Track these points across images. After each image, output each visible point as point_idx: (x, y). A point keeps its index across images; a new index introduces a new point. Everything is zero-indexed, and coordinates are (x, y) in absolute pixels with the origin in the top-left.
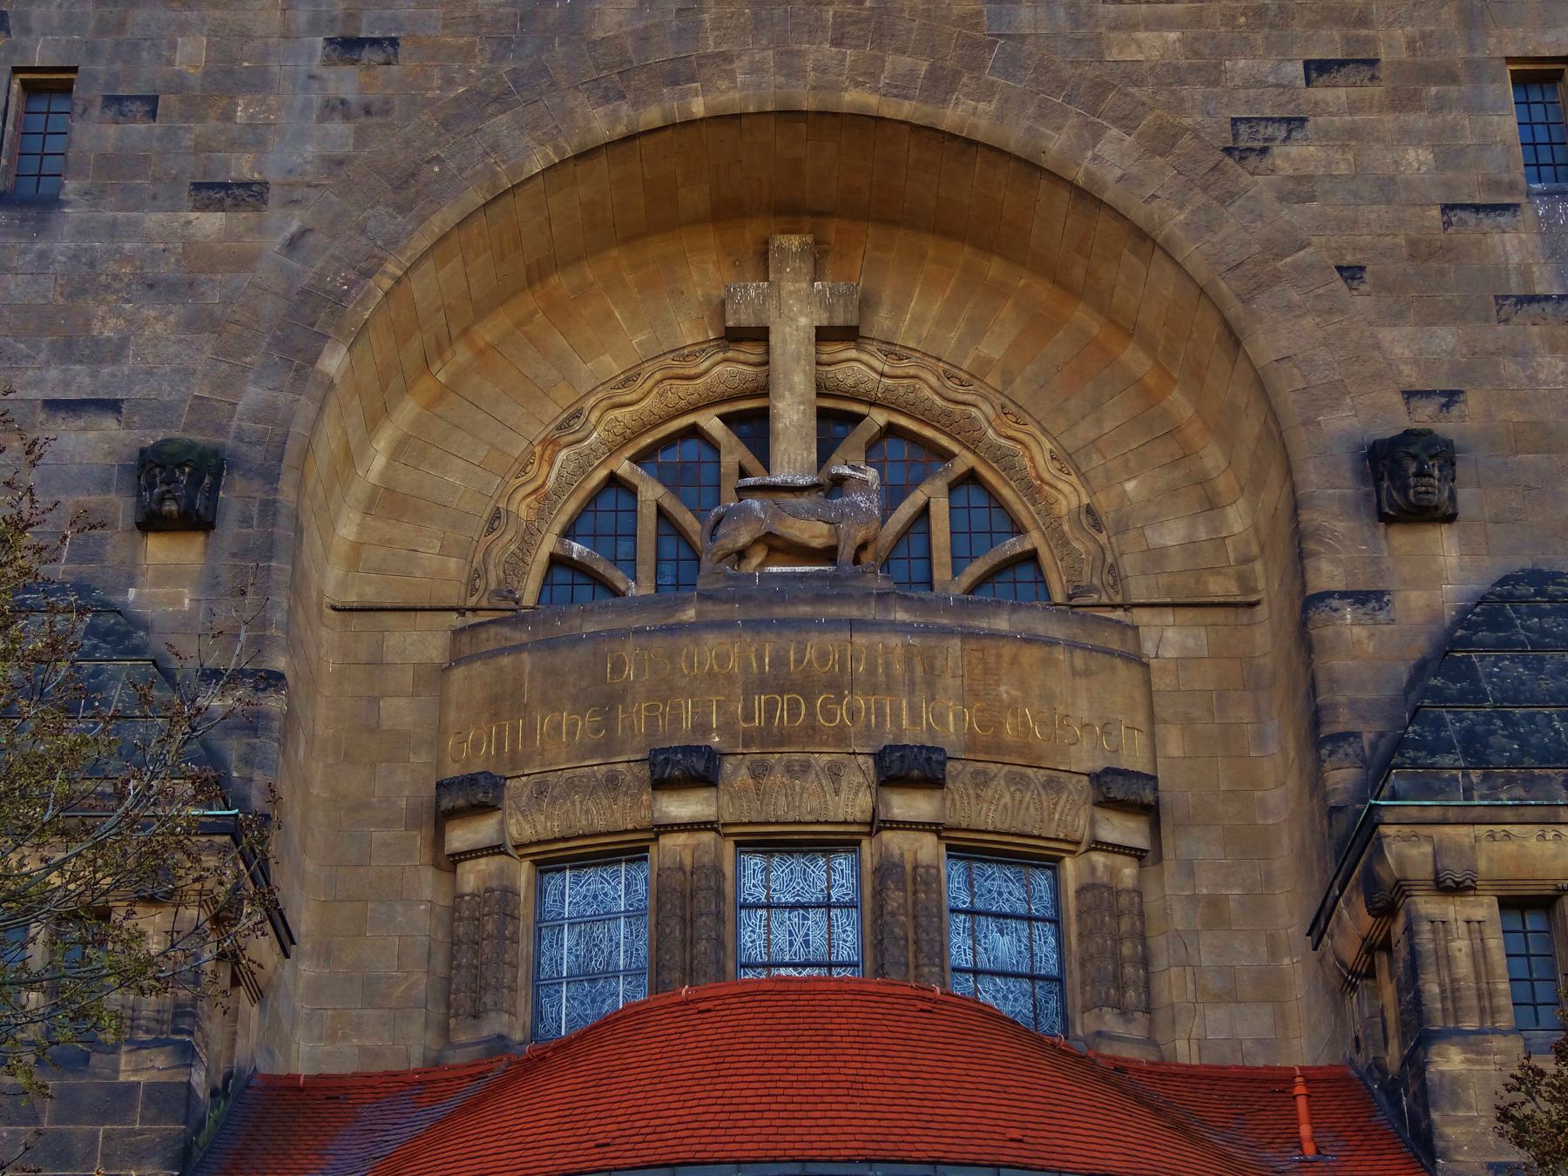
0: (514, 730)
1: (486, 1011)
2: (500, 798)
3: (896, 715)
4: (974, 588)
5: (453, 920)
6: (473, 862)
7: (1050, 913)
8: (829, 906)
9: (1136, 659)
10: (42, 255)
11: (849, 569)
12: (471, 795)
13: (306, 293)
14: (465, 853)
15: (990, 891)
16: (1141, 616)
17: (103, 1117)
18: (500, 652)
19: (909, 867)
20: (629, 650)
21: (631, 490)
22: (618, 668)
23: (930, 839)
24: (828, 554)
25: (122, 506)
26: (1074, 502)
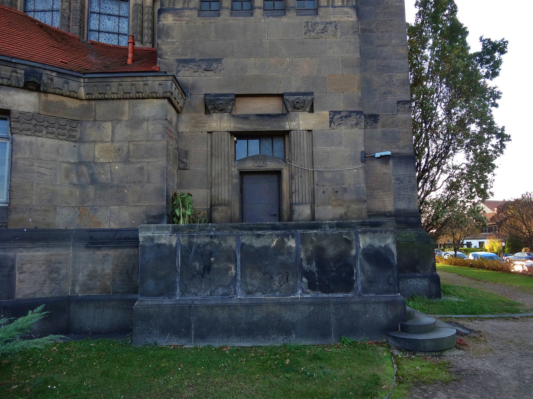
7: (126, 15)
8: (53, 11)
15: (106, 7)
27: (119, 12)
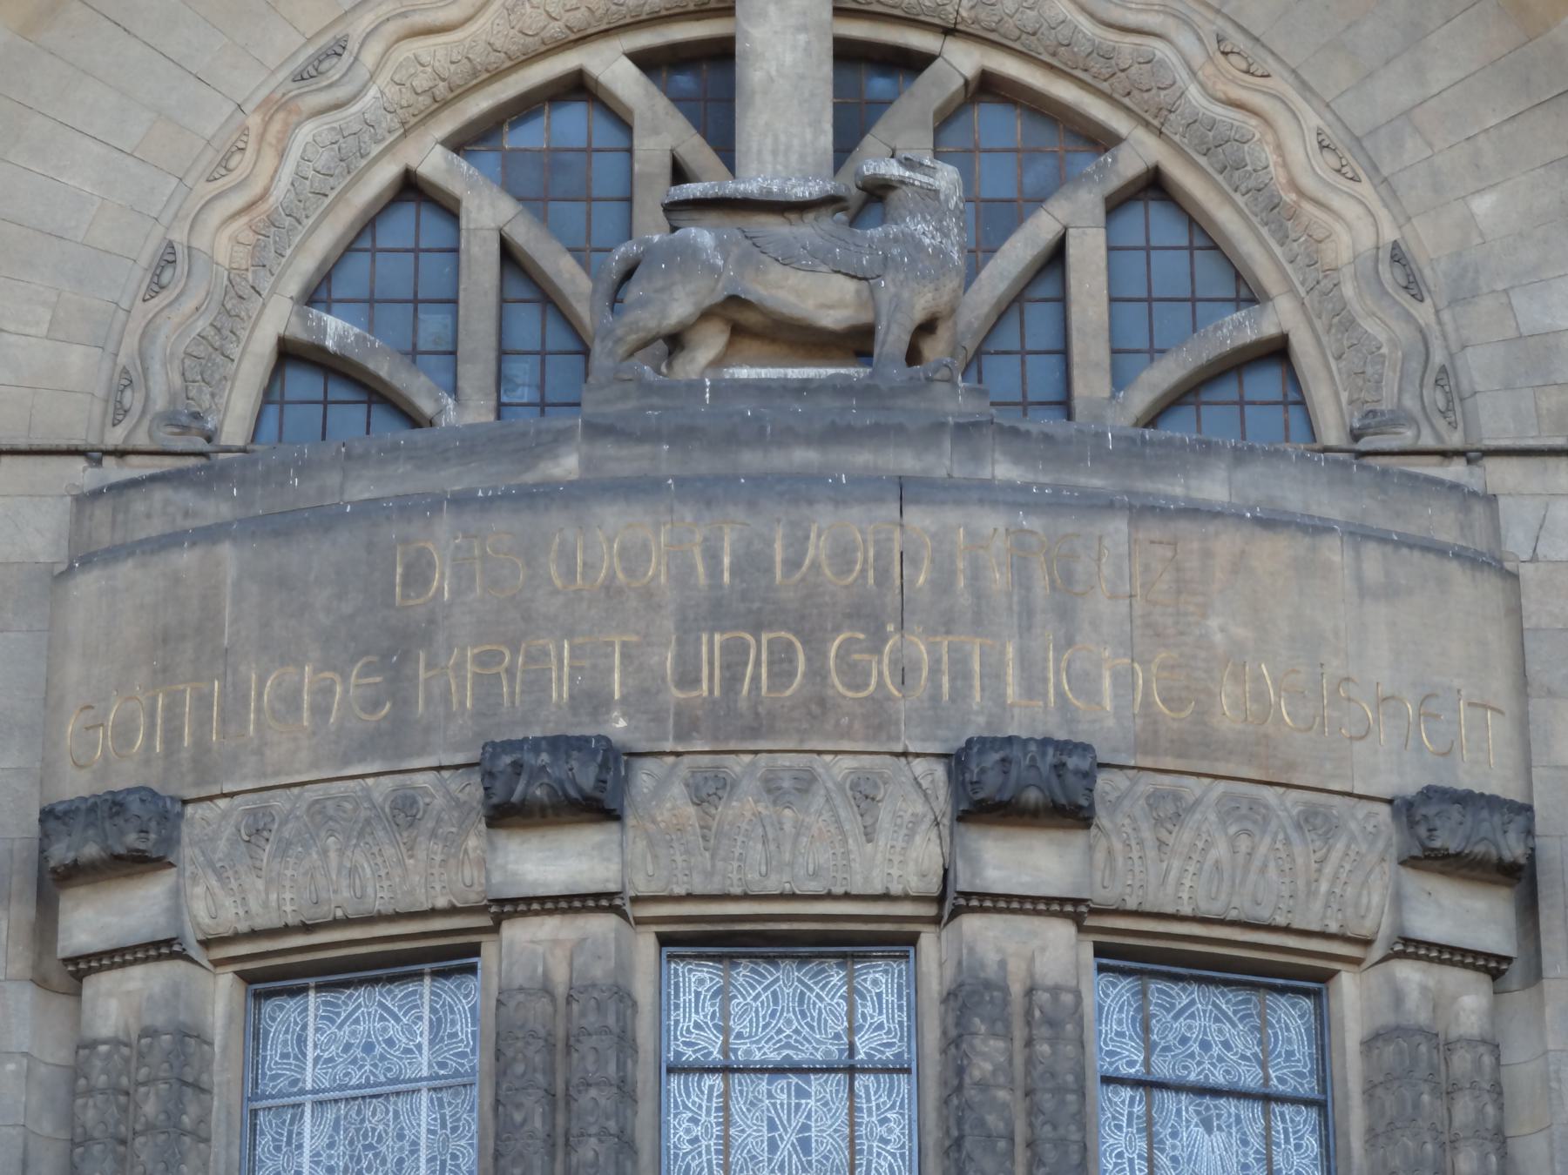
0: (203, 701)
2: (172, 841)
3: (994, 676)
4: (1153, 418)
5: (74, 1094)
6: (116, 974)
7: (1308, 1087)
8: (851, 1070)
9: (1489, 562)
11: (898, 373)
12: (115, 837)
14: (98, 956)
15: (1184, 1041)
16: (1500, 474)
18: (171, 541)
19: (1017, 989)
20: (442, 539)
21: (449, 209)
22: (418, 574)
23: (1061, 931)
24: (856, 343)
26: (1367, 241)
27: (1264, 1066)
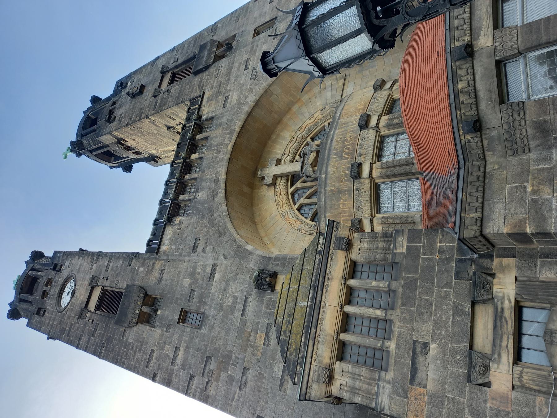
1: (413, 220)
10: (213, 317)
13: (235, 254)
17: (418, 256)
24: (318, 152)
25: (268, 296)
